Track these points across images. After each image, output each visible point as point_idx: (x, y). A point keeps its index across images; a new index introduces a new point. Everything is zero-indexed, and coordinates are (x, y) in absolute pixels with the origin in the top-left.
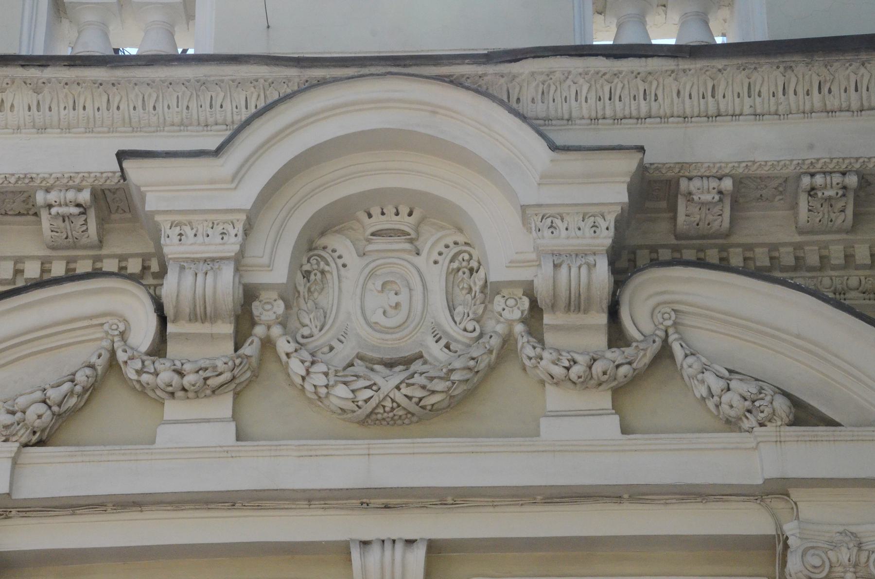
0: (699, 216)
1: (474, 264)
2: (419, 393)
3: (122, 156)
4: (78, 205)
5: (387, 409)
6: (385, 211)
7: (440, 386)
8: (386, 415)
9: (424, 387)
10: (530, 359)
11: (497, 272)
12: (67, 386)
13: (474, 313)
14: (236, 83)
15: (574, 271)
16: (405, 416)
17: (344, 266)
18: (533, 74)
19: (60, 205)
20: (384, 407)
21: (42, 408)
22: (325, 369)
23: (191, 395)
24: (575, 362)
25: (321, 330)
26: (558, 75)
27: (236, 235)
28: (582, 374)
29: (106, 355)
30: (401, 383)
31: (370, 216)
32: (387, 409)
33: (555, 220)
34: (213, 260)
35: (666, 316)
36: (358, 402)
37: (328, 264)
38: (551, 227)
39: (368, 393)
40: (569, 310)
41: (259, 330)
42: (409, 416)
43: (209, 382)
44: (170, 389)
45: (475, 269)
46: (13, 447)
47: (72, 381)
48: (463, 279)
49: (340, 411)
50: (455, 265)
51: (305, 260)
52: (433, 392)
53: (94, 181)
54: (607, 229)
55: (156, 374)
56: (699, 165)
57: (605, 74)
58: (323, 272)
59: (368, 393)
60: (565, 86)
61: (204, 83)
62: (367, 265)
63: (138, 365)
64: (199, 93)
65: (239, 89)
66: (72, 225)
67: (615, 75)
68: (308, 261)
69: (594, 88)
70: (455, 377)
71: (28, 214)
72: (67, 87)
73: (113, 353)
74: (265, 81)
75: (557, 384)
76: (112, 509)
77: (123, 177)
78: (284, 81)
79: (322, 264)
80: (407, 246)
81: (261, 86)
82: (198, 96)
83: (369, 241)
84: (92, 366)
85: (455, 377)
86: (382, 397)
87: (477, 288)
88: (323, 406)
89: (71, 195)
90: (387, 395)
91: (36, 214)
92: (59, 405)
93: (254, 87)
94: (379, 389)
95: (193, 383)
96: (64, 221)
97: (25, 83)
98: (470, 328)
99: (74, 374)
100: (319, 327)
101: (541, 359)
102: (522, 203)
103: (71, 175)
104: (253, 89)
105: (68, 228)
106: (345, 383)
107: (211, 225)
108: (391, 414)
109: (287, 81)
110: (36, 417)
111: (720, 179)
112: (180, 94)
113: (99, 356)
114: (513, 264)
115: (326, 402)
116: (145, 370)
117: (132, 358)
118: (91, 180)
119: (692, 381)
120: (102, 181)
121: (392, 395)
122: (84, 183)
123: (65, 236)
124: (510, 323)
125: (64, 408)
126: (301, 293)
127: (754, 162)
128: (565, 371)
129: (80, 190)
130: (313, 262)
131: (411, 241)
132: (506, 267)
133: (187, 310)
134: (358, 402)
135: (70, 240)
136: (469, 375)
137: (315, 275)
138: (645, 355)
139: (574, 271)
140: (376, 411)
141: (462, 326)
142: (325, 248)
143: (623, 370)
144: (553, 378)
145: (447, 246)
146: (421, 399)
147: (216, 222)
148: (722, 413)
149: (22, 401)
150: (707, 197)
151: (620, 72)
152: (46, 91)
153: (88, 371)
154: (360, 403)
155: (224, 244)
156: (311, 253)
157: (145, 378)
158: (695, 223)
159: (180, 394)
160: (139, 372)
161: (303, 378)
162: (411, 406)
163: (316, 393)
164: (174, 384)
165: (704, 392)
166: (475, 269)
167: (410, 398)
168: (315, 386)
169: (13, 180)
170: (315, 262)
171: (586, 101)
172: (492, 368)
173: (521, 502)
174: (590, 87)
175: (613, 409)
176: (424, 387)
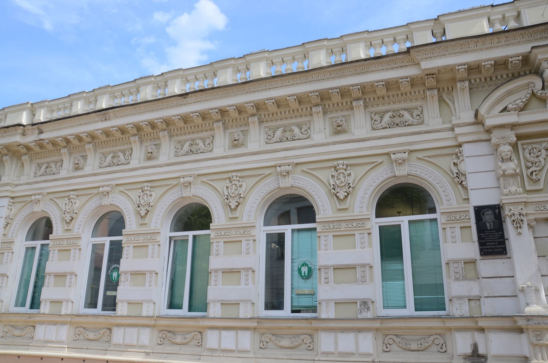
4: (519, 60)
12: (526, 98)
21: (522, 103)
29: (531, 91)
73: (533, 90)
84: (529, 94)
92: (525, 102)
113: (530, 91)
157: (543, 95)
160: (541, 94)
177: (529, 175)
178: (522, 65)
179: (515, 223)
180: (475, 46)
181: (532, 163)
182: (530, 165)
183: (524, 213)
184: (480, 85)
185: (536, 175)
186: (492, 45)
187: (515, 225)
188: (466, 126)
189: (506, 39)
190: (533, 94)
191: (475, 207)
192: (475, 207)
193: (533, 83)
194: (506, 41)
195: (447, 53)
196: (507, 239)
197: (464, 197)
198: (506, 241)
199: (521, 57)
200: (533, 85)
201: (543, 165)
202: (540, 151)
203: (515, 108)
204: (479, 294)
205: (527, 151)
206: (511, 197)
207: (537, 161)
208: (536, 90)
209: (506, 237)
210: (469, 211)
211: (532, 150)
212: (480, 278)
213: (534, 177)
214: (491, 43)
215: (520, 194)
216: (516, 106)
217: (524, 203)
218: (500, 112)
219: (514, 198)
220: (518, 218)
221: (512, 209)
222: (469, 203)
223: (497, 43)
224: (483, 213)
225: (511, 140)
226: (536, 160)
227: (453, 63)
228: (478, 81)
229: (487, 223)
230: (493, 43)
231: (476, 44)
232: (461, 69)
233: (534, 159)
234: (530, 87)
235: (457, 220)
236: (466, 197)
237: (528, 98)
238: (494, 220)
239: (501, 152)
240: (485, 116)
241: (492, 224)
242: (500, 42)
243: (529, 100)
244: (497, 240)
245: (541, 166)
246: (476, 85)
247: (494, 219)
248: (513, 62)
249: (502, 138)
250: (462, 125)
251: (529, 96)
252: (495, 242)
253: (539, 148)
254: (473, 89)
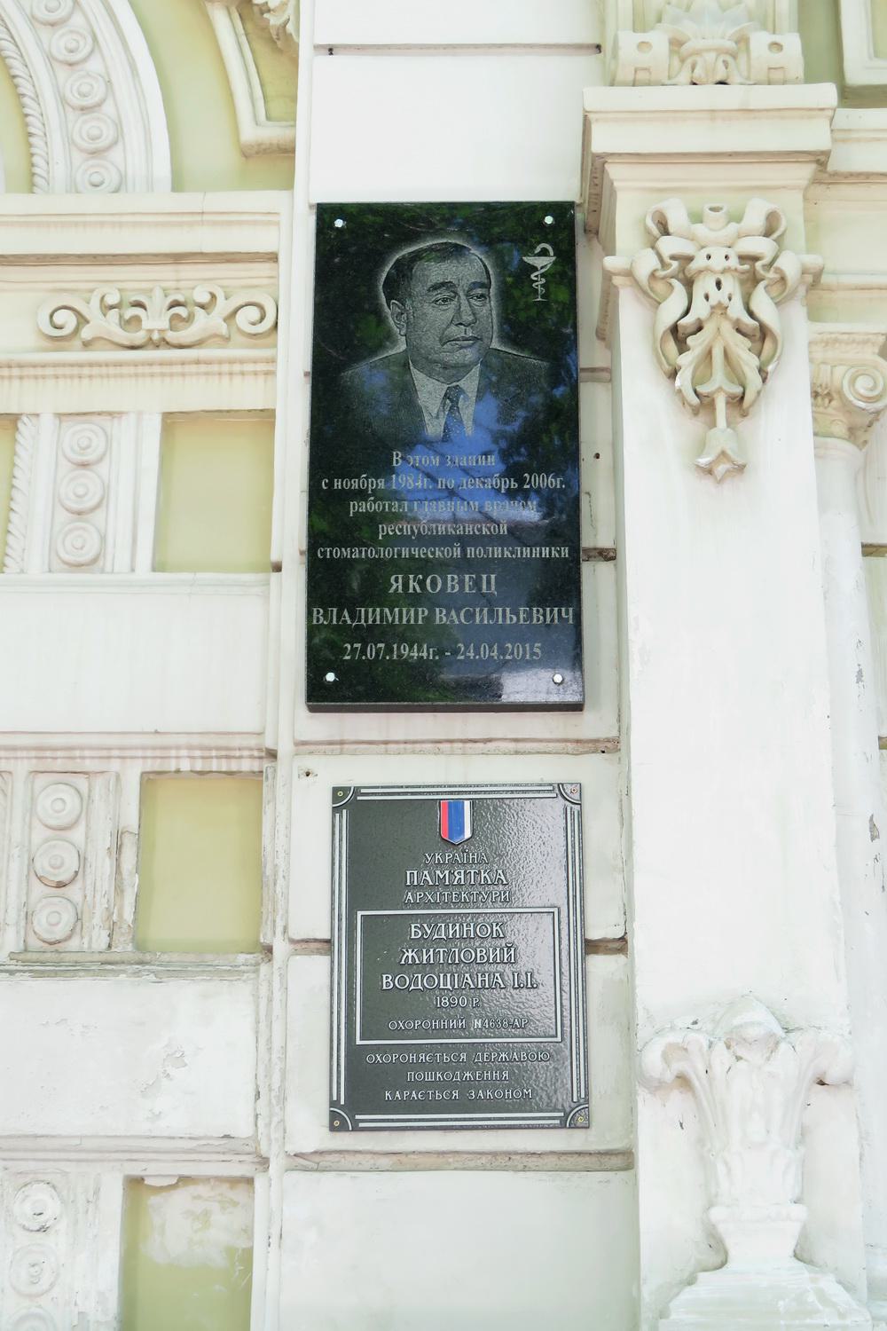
179: (686, 361)
183: (789, 264)
187: (683, 380)
191: (325, 213)
192: (325, 213)
196: (608, 555)
197: (250, 133)
198: (594, 577)
204: (243, 1129)
206: (681, 96)
209: (594, 535)
210: (273, 258)
212: (280, 947)
215: (772, 78)
220: (720, 309)
221: (677, 219)
222: (288, 183)
224: (404, 271)
229: (419, 377)
235: (150, 344)
236: (272, 133)
238: (495, 344)
241: (470, 383)
244: (497, 552)
247: (506, 338)
252: (485, 565)
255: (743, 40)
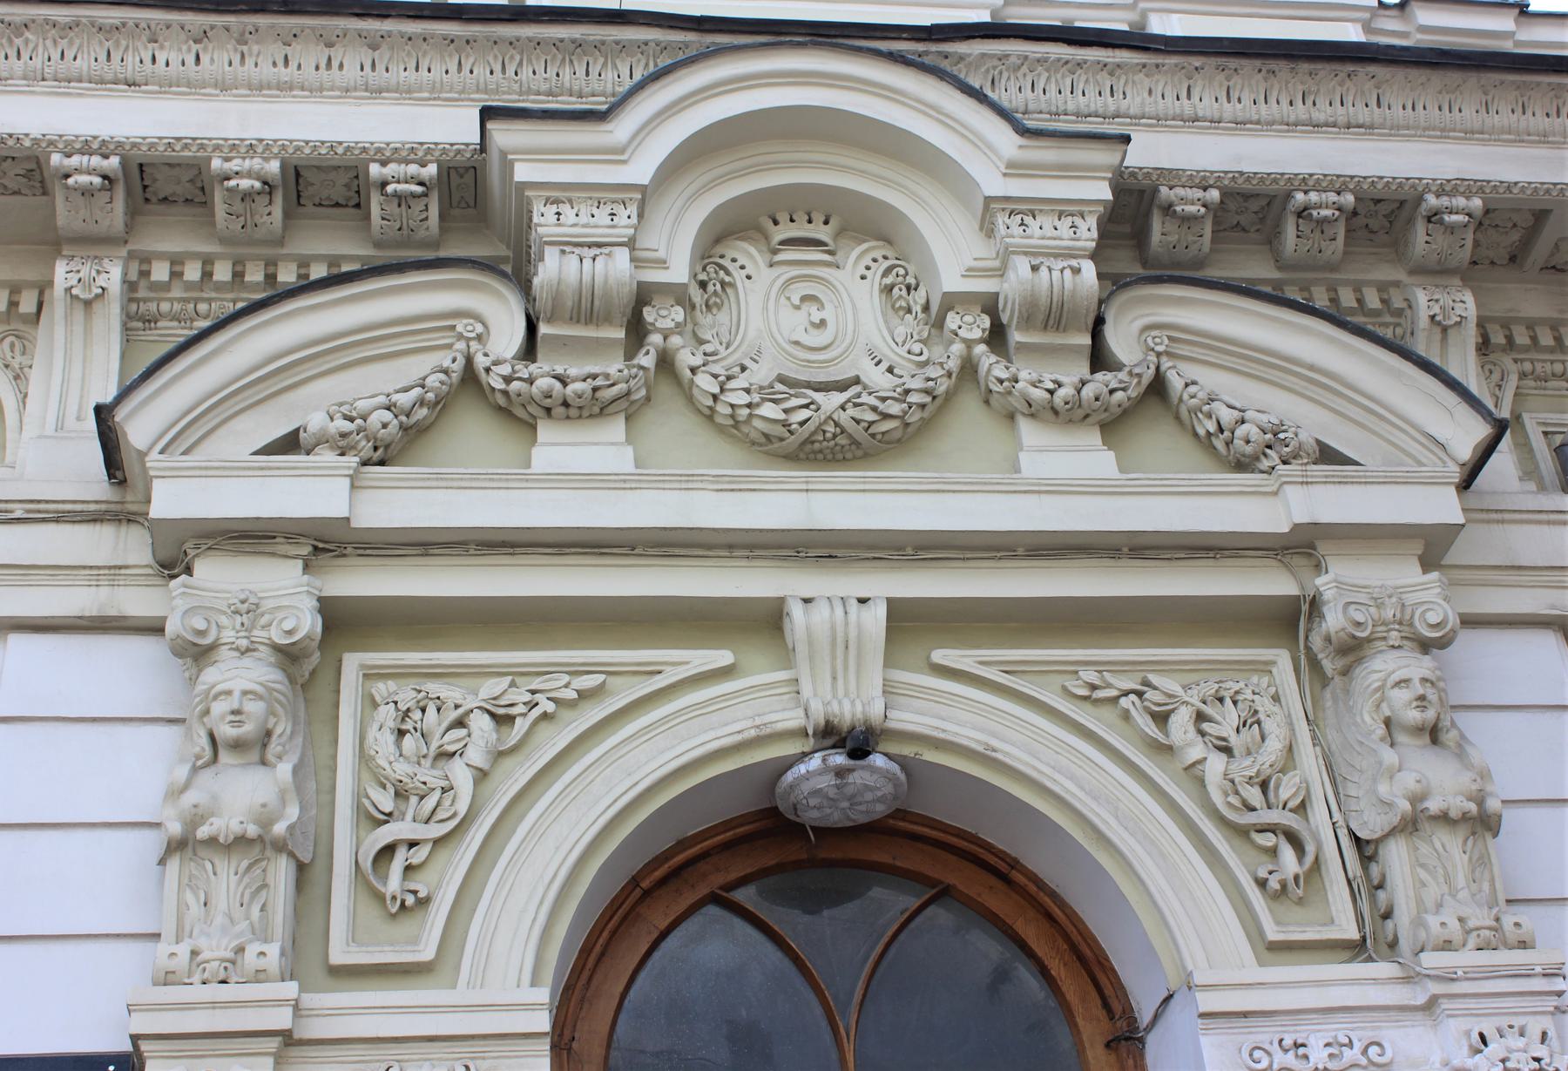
0: (1177, 236)
1: (911, 280)
2: (871, 417)
3: (487, 114)
4: (421, 184)
5: (829, 435)
6: (794, 217)
7: (895, 408)
8: (825, 443)
9: (874, 409)
10: (1001, 381)
11: (953, 282)
12: (418, 390)
13: (919, 334)
14: (620, 47)
15: (1056, 274)
16: (848, 447)
17: (749, 277)
18: (983, 55)
19: (398, 182)
20: (824, 432)
21: (387, 416)
22: (747, 385)
23: (573, 412)
24: (1060, 386)
25: (727, 348)
26: (1013, 59)
27: (629, 217)
28: (1070, 399)
29: (461, 361)
30: (846, 402)
31: (776, 223)
32: (829, 435)
33: (1025, 218)
34: (599, 245)
35: (1157, 340)
36: (790, 425)
37: (728, 273)
38: (1022, 224)
39: (805, 414)
40: (1046, 327)
41: (655, 339)
42: (853, 447)
43: (599, 394)
44: (547, 402)
45: (913, 286)
46: (352, 460)
47: (423, 387)
48: (901, 296)
49: (763, 440)
50: (889, 280)
51: (699, 268)
52: (886, 416)
53: (441, 155)
54: (1089, 230)
55: (531, 381)
56: (1181, 172)
57: (1067, 62)
58: (723, 284)
59: (805, 414)
60: (1020, 74)
61: (580, 45)
62: (778, 277)
63: (505, 370)
64: (573, 58)
65: (624, 54)
66: (409, 211)
67: (1079, 64)
68: (704, 269)
69: (1053, 80)
70: (913, 398)
71: (347, 206)
72: (410, 43)
73: (469, 360)
74: (657, 45)
75: (1032, 415)
76: (476, 550)
77: (483, 146)
78: (680, 45)
79: (722, 273)
80: (826, 257)
81: (651, 53)
82: (571, 61)
83: (775, 252)
84: (446, 372)
85: (913, 398)
86: (823, 417)
87: (917, 308)
88: (739, 435)
89: (413, 169)
90: (830, 417)
91: (358, 206)
93: (642, 53)
94: (818, 409)
95: (580, 392)
96: (399, 206)
97: (360, 36)
98: (918, 351)
99: (424, 379)
100: (724, 345)
101: (1017, 382)
102: (987, 194)
103: (415, 146)
104: (640, 55)
105: (404, 214)
106: (774, 401)
107: (596, 204)
108: (832, 443)
109: (687, 45)
110: (380, 425)
111: (1205, 189)
112: (549, 58)
113: (454, 360)
114: (971, 273)
115: (745, 429)
116: (517, 375)
117: (496, 363)
118: (437, 154)
119: (1193, 416)
120: (452, 154)
121: (835, 417)
122: (429, 157)
123: (398, 227)
124: (969, 344)
125: (413, 419)
126: (698, 306)
127: (1241, 173)
128: (1048, 396)
129: (423, 166)
130: (710, 269)
131: (831, 253)
132: (963, 276)
133: (570, 304)
134: (790, 425)
135: (405, 232)
136: (928, 399)
137: (714, 285)
138: (1139, 383)
139: (1056, 274)
140: (813, 438)
141: (907, 347)
142: (722, 257)
143: (1119, 395)
144: (1030, 405)
145: (875, 260)
146: (871, 423)
147: (602, 201)
148: (1232, 452)
149: (362, 405)
150: (1192, 209)
151: (1085, 62)
152: (384, 47)
153: (442, 376)
154: (794, 426)
155: (613, 227)
156: (707, 261)
157: (516, 386)
158: (1171, 246)
159: (562, 410)
160: (508, 380)
161: (715, 397)
162: (857, 431)
163: (732, 416)
164: (554, 394)
165: (1212, 427)
166: (913, 286)
167: (858, 422)
168: (732, 406)
169: (340, 150)
170: (712, 270)
171: (1044, 93)
172: (950, 395)
173: (999, 555)
174: (1048, 79)
175: (1104, 445)
176: (874, 409)
177: (367, 864)
178: (442, 217)
180: (191, 59)
181: (401, 794)
182: (386, 802)
184: (202, 307)
185: (409, 869)
186: (284, 74)
188: (44, 520)
189: (366, 56)
190: (470, 377)
193: (478, 318)
194: (368, 68)
195: (18, 66)
199: (432, 169)
200: (479, 328)
201: (462, 807)
202: (460, 723)
203: (344, 435)
205: (387, 714)
206: (198, 993)
207: (432, 782)
208: (486, 355)
211: (417, 715)
213: (394, 882)
214: (281, 63)
215: (259, 976)
216: (347, 426)
217: (273, 1044)
218: (255, 453)
219: (214, 1005)
223: (317, 68)
225: (288, 626)
226: (429, 775)
227: (36, 133)
228: (192, 272)
230: (293, 64)
231: (195, 47)
232: (78, 171)
233: (417, 769)
234: (460, 337)
237: (431, 396)
239: (208, 692)
240: (154, 460)
242: (335, 64)
243: (441, 405)
245: (454, 815)
246: (180, 300)
248: (390, 188)
249: (236, 612)
250: (18, 514)
251: (437, 384)
253: (457, 707)
254: (159, 324)
255: (240, 950)
